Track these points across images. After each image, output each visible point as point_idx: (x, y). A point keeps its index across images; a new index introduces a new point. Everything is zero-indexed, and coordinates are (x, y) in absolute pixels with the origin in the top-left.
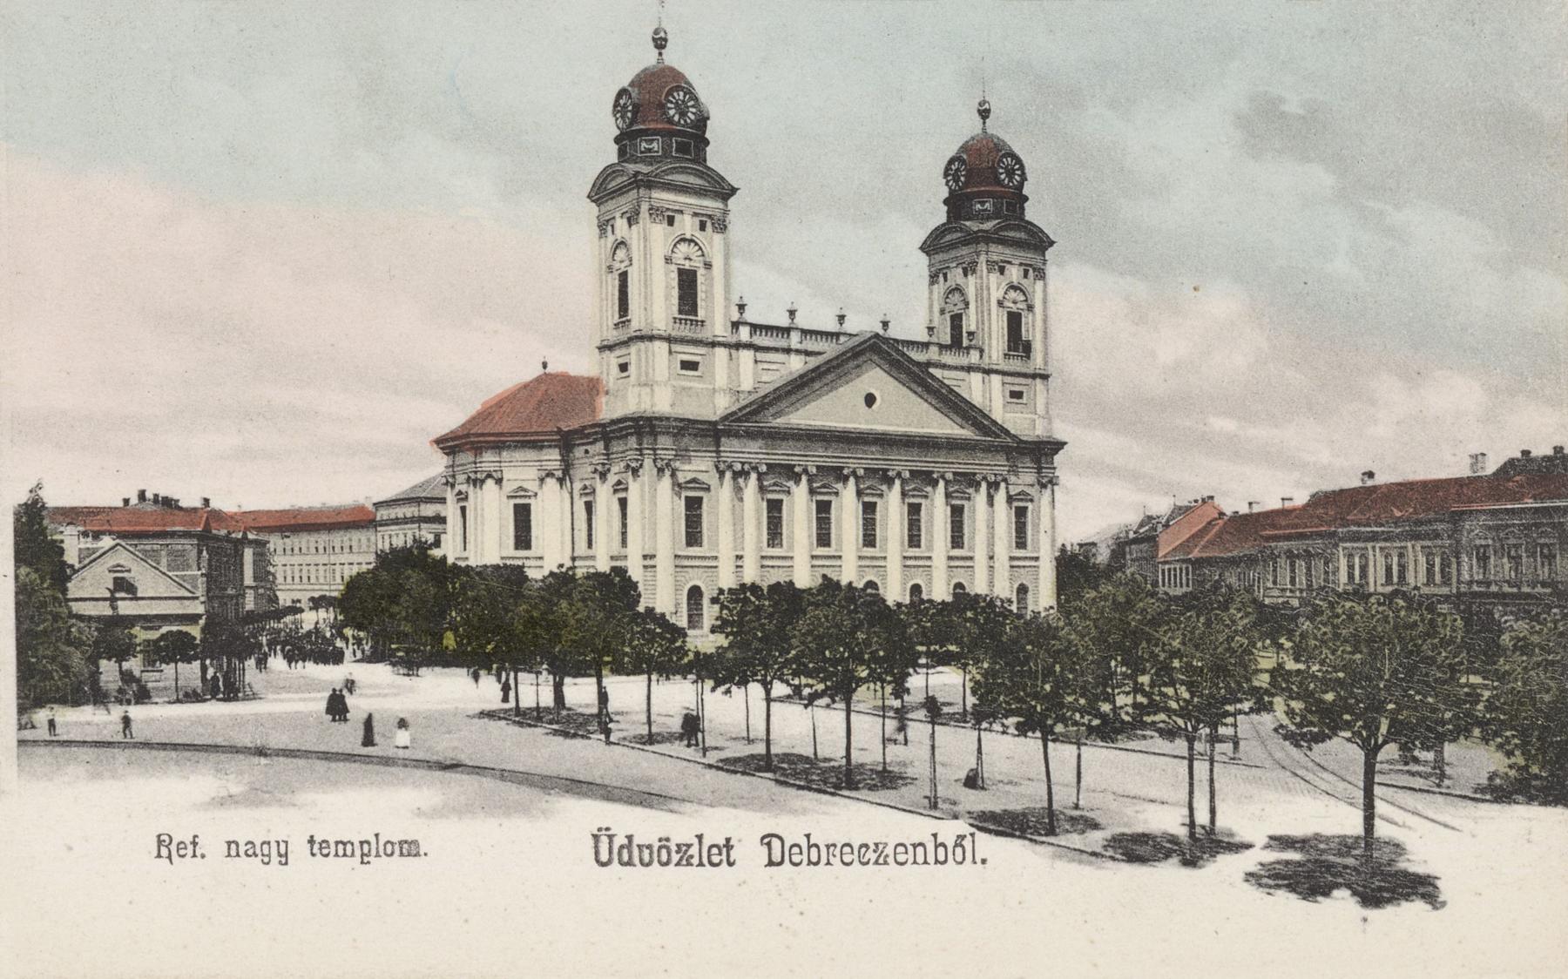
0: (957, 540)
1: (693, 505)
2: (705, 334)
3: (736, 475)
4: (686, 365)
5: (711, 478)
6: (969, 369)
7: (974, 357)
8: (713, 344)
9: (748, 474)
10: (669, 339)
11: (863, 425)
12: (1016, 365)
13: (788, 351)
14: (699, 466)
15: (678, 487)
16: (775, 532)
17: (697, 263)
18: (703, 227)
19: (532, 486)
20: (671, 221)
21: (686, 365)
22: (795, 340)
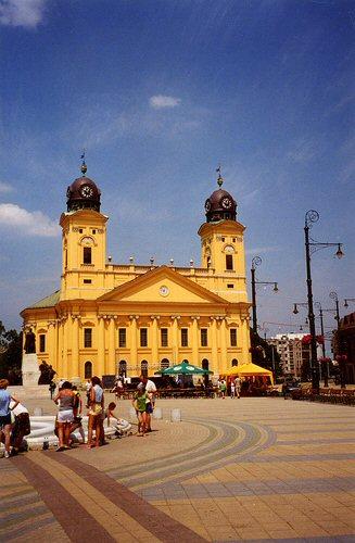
0: (204, 342)
1: (88, 332)
2: (96, 269)
3: (105, 320)
4: (86, 281)
5: (95, 321)
6: (208, 277)
7: (211, 273)
8: (97, 273)
9: (109, 320)
10: (79, 272)
11: (161, 299)
12: (229, 275)
13: (128, 274)
14: (91, 317)
15: (80, 325)
16: (122, 341)
17: (91, 245)
18: (94, 232)
19: (46, 328)
20: (81, 231)
21: (86, 281)
22: (132, 270)
